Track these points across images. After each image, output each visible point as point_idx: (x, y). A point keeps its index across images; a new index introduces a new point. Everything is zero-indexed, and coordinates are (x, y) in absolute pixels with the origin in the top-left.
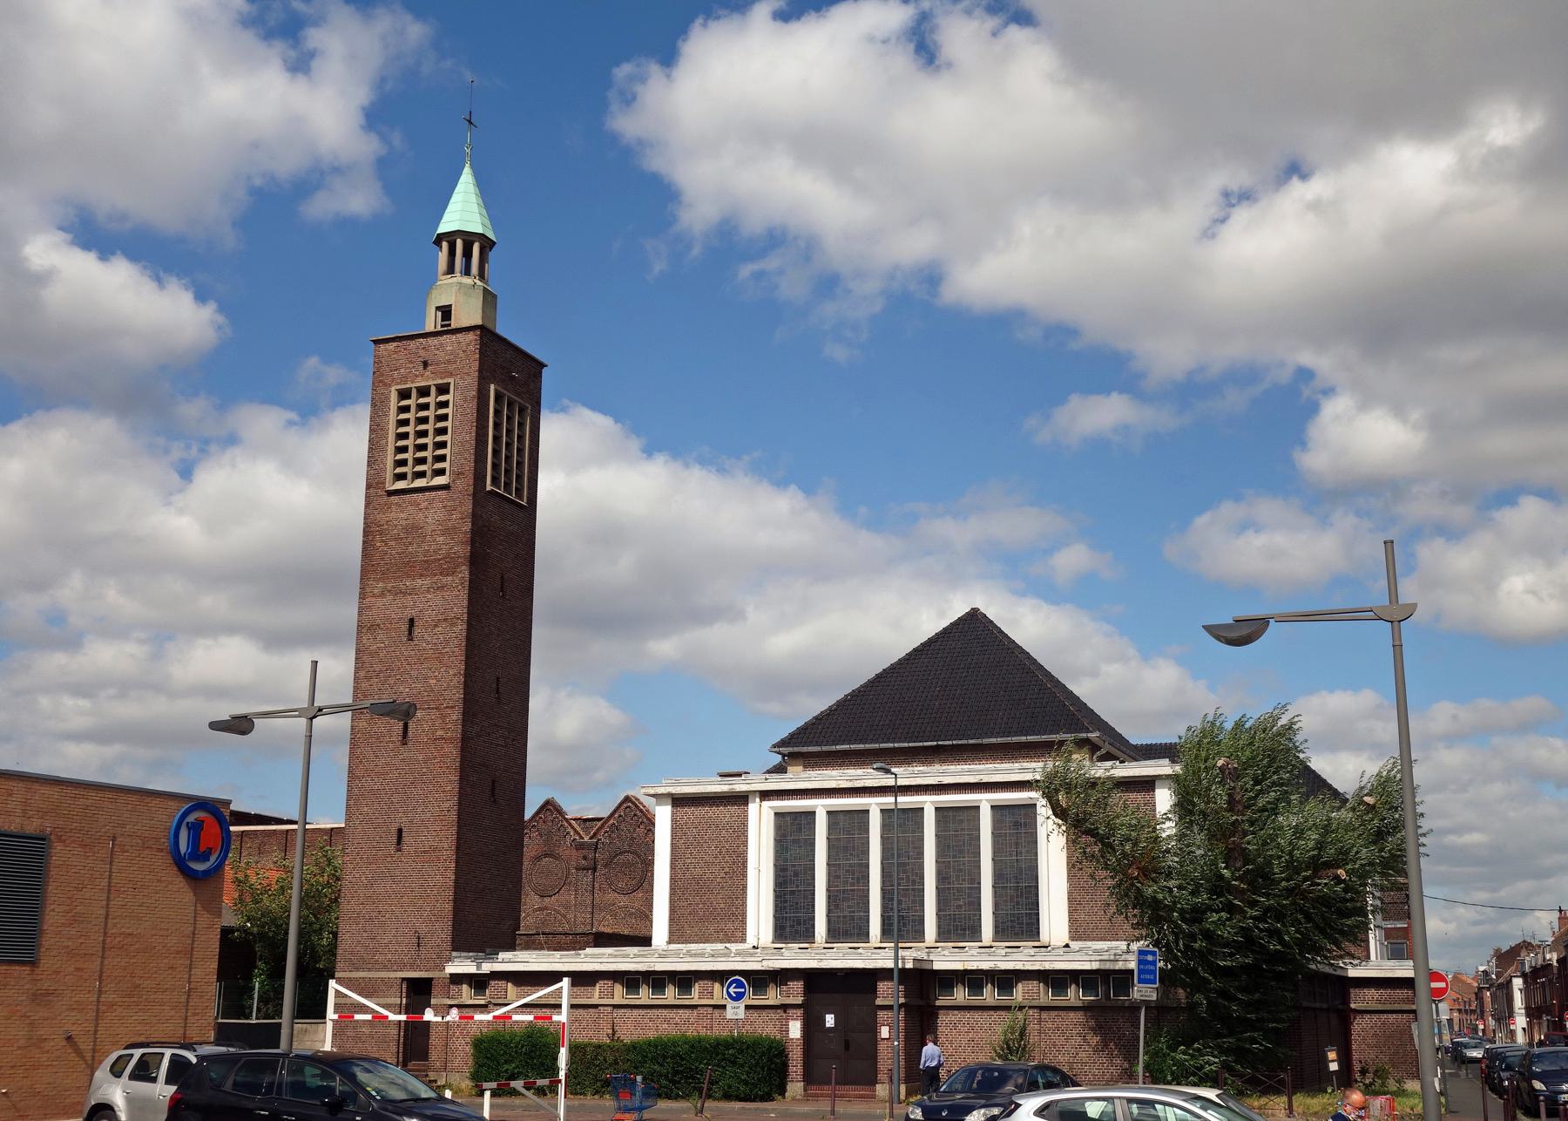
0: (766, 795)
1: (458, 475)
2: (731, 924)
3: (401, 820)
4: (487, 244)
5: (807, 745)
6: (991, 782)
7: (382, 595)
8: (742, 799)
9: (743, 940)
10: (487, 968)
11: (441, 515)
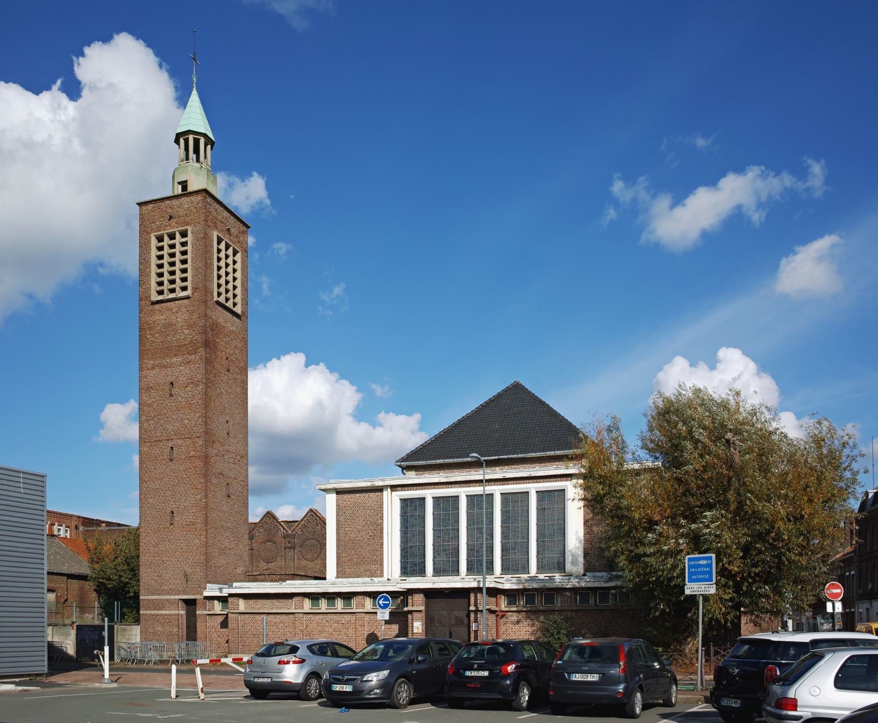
0: (394, 488)
1: (195, 289)
2: (375, 567)
3: (172, 506)
4: (209, 141)
5: (417, 460)
6: (531, 481)
7: (153, 368)
8: (380, 489)
9: (382, 575)
10: (226, 592)
11: (186, 316)
